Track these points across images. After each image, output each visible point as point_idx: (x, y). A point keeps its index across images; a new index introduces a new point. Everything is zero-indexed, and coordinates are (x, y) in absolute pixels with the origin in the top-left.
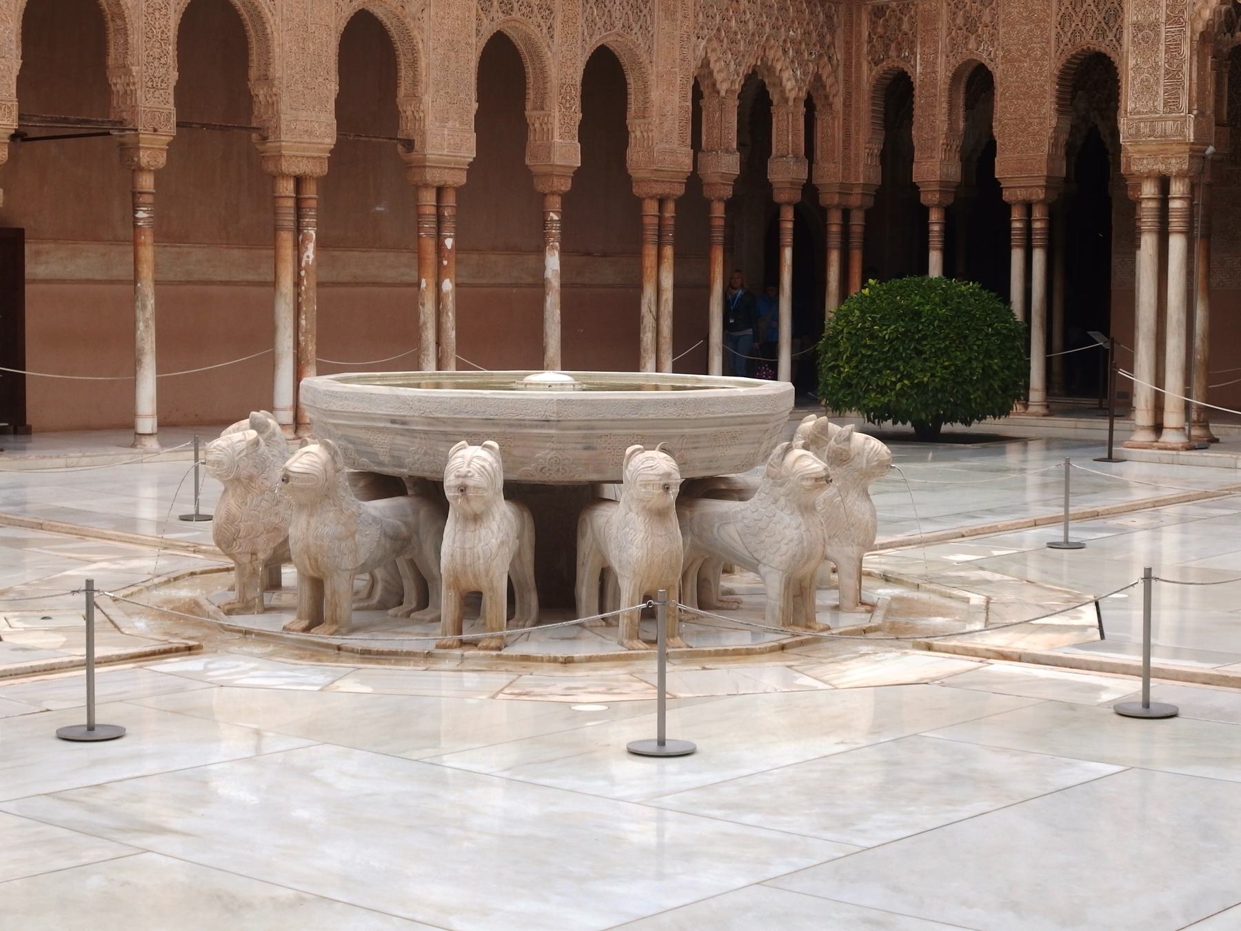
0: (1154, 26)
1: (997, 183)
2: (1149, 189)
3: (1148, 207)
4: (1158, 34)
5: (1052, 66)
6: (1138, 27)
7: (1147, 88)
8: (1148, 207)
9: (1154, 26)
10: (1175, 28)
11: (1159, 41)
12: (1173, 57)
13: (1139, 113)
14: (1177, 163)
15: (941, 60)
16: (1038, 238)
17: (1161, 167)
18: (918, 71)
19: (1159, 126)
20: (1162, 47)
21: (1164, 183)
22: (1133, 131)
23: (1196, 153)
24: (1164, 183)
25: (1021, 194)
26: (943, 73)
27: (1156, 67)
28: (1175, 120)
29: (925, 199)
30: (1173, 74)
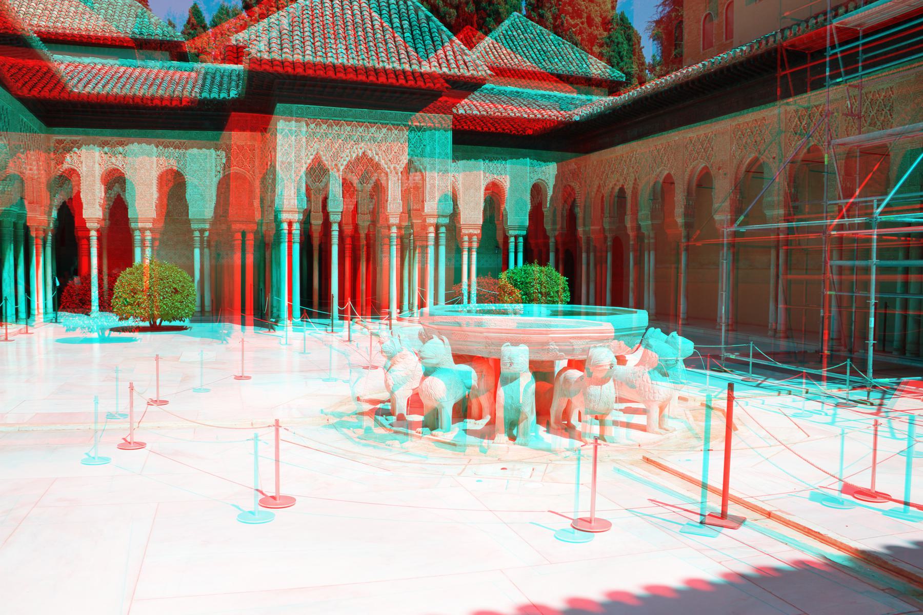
0: (290, 163)
1: (128, 219)
2: (285, 226)
5: (155, 174)
6: (283, 163)
9: (290, 163)
15: (97, 166)
16: (148, 243)
18: (83, 170)
21: (290, 224)
24: (290, 224)
25: (140, 225)
26: (98, 172)
29: (88, 225)
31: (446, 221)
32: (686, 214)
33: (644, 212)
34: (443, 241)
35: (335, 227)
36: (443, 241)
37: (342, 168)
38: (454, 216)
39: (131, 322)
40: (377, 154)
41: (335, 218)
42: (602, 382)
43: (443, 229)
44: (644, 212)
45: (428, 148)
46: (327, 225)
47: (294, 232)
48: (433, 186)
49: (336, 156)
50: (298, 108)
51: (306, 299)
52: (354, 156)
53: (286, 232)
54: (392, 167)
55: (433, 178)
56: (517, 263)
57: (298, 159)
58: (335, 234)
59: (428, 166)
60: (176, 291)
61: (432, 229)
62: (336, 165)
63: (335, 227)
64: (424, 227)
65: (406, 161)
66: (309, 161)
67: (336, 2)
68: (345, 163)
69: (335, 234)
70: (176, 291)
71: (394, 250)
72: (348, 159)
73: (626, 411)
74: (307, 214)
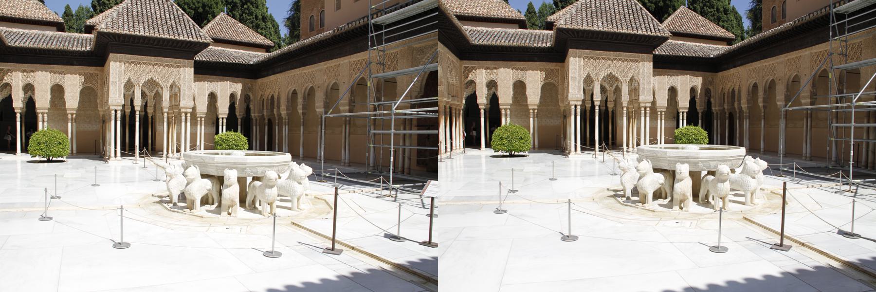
31: (649, 105)
32: (764, 101)
33: (744, 101)
35: (597, 108)
38: (654, 103)
39: (500, 153)
41: (597, 103)
42: (723, 181)
44: (744, 101)
46: (593, 107)
49: (597, 74)
51: (583, 142)
56: (683, 125)
58: (597, 111)
60: (522, 138)
63: (597, 108)
64: (639, 108)
67: (598, 1)
69: (597, 111)
70: (522, 138)
71: (625, 118)
73: (735, 195)
74: (584, 101)
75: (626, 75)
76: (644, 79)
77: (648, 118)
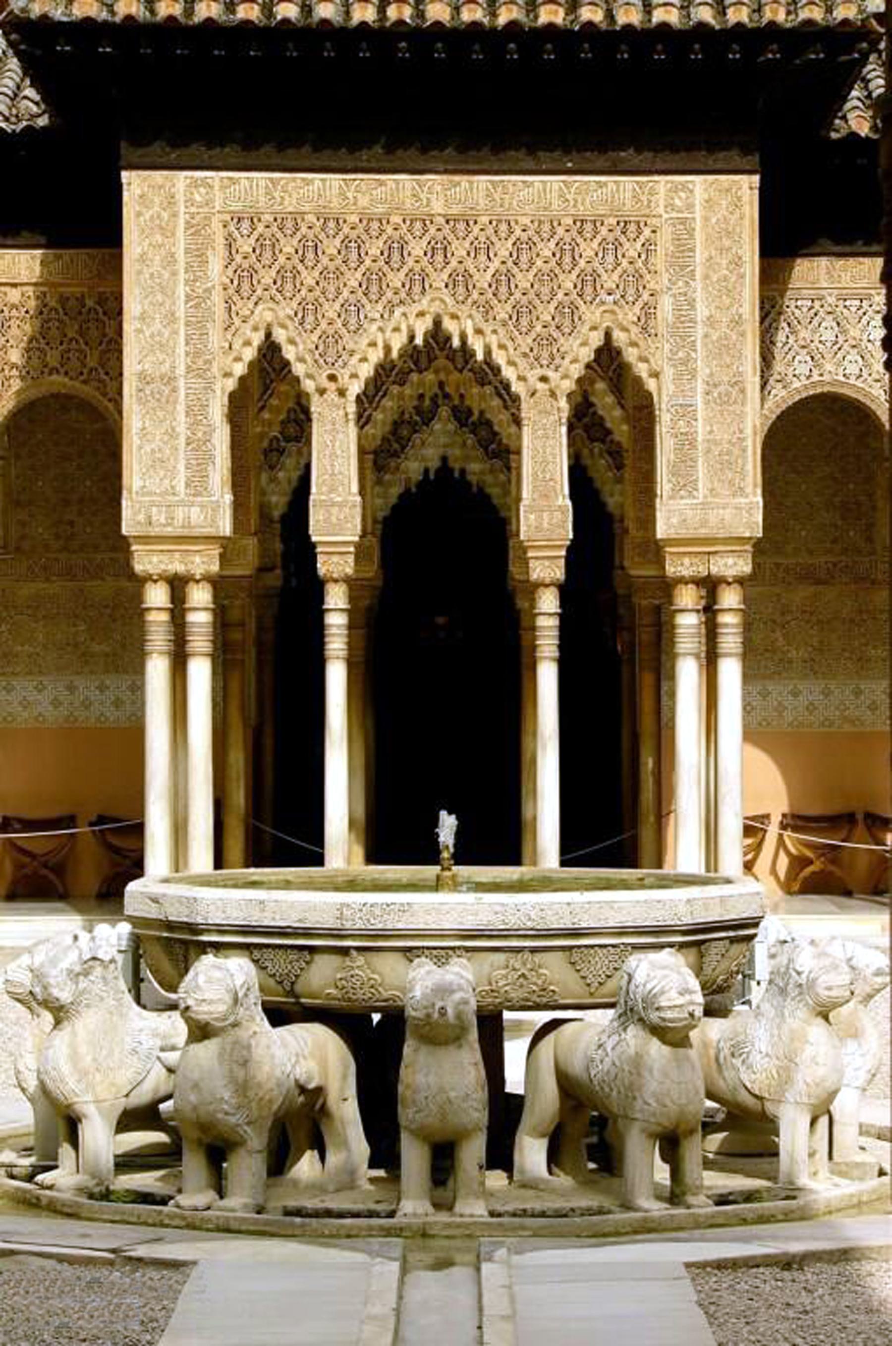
0: (170, 380)
2: (157, 596)
3: (158, 620)
4: (174, 390)
7: (158, 462)
8: (158, 620)
10: (199, 384)
11: (176, 402)
12: (198, 423)
13: (150, 494)
14: (204, 562)
17: (177, 567)
19: (180, 514)
20: (181, 408)
22: (141, 517)
23: (228, 549)
27: (172, 434)
28: (202, 506)
30: (198, 446)
34: (730, 641)
36: (730, 641)
37: (355, 388)
40: (479, 332)
43: (730, 598)
45: (666, 306)
47: (191, 617)
48: (687, 442)
50: (195, 184)
52: (398, 343)
53: (164, 617)
54: (532, 376)
55: (686, 412)
57: (199, 369)
59: (668, 373)
61: (687, 597)
62: (332, 378)
64: (667, 587)
65: (587, 354)
66: (240, 369)
68: (366, 371)
72: (376, 356)
75: (546, 348)
76: (686, 370)
77: (730, 671)
